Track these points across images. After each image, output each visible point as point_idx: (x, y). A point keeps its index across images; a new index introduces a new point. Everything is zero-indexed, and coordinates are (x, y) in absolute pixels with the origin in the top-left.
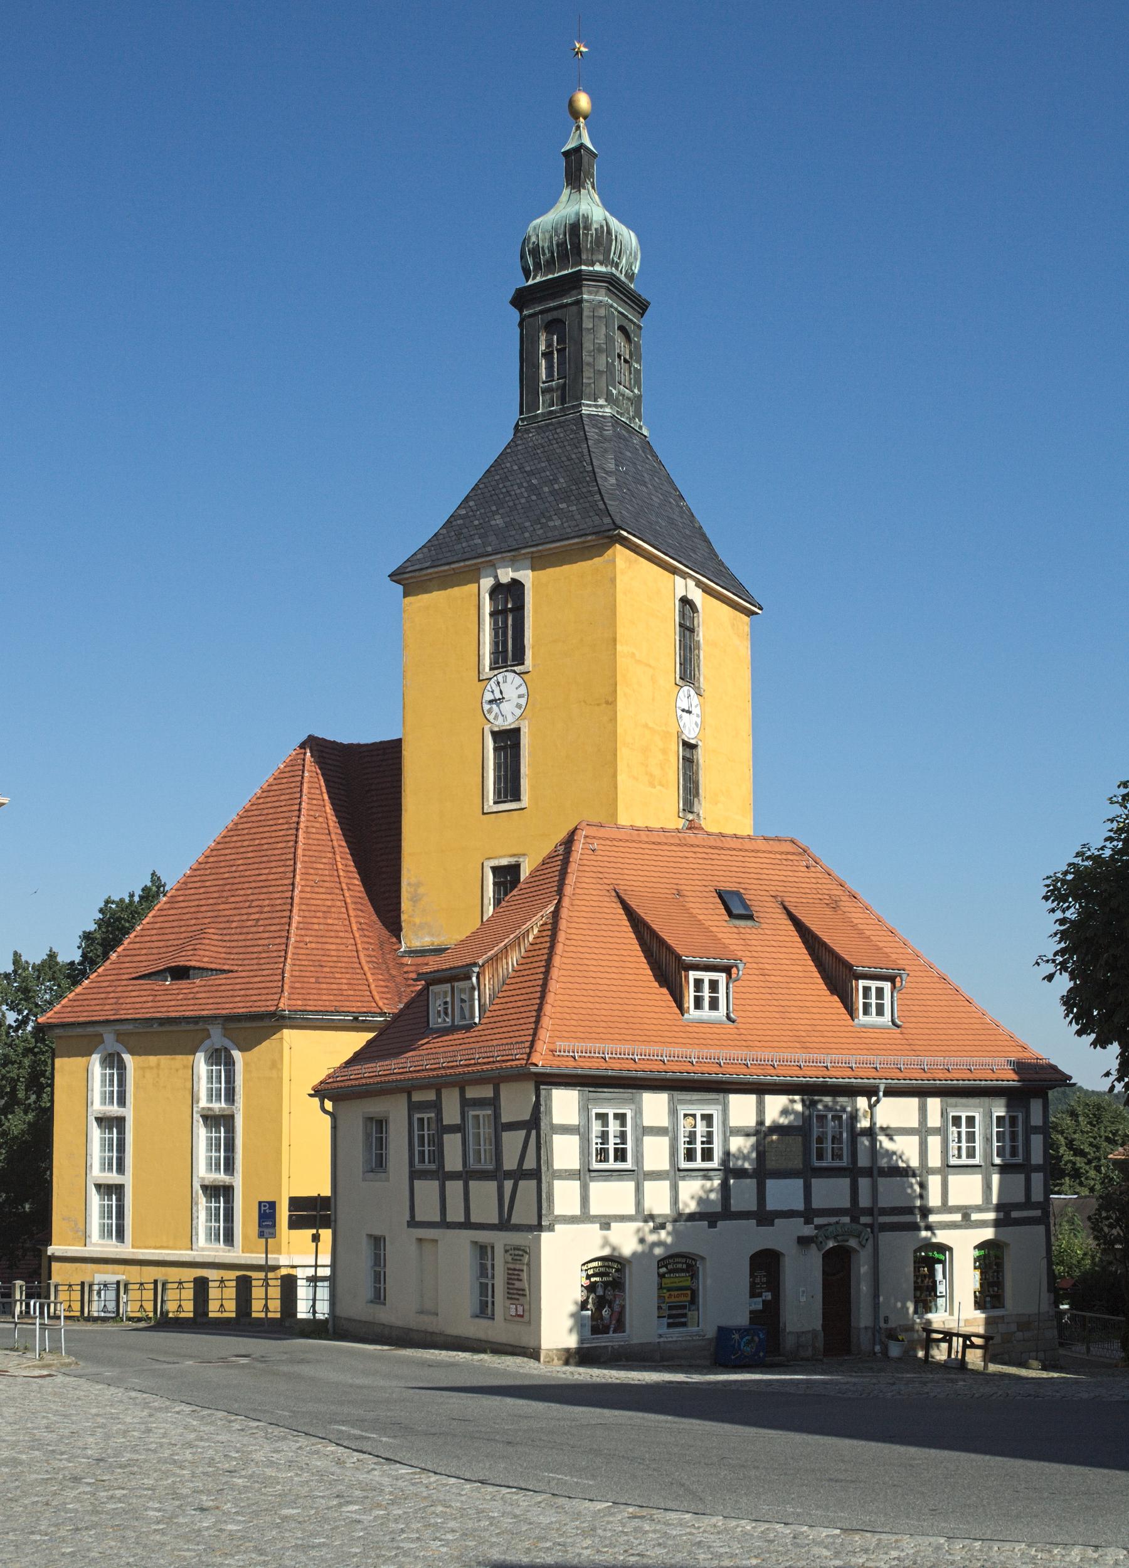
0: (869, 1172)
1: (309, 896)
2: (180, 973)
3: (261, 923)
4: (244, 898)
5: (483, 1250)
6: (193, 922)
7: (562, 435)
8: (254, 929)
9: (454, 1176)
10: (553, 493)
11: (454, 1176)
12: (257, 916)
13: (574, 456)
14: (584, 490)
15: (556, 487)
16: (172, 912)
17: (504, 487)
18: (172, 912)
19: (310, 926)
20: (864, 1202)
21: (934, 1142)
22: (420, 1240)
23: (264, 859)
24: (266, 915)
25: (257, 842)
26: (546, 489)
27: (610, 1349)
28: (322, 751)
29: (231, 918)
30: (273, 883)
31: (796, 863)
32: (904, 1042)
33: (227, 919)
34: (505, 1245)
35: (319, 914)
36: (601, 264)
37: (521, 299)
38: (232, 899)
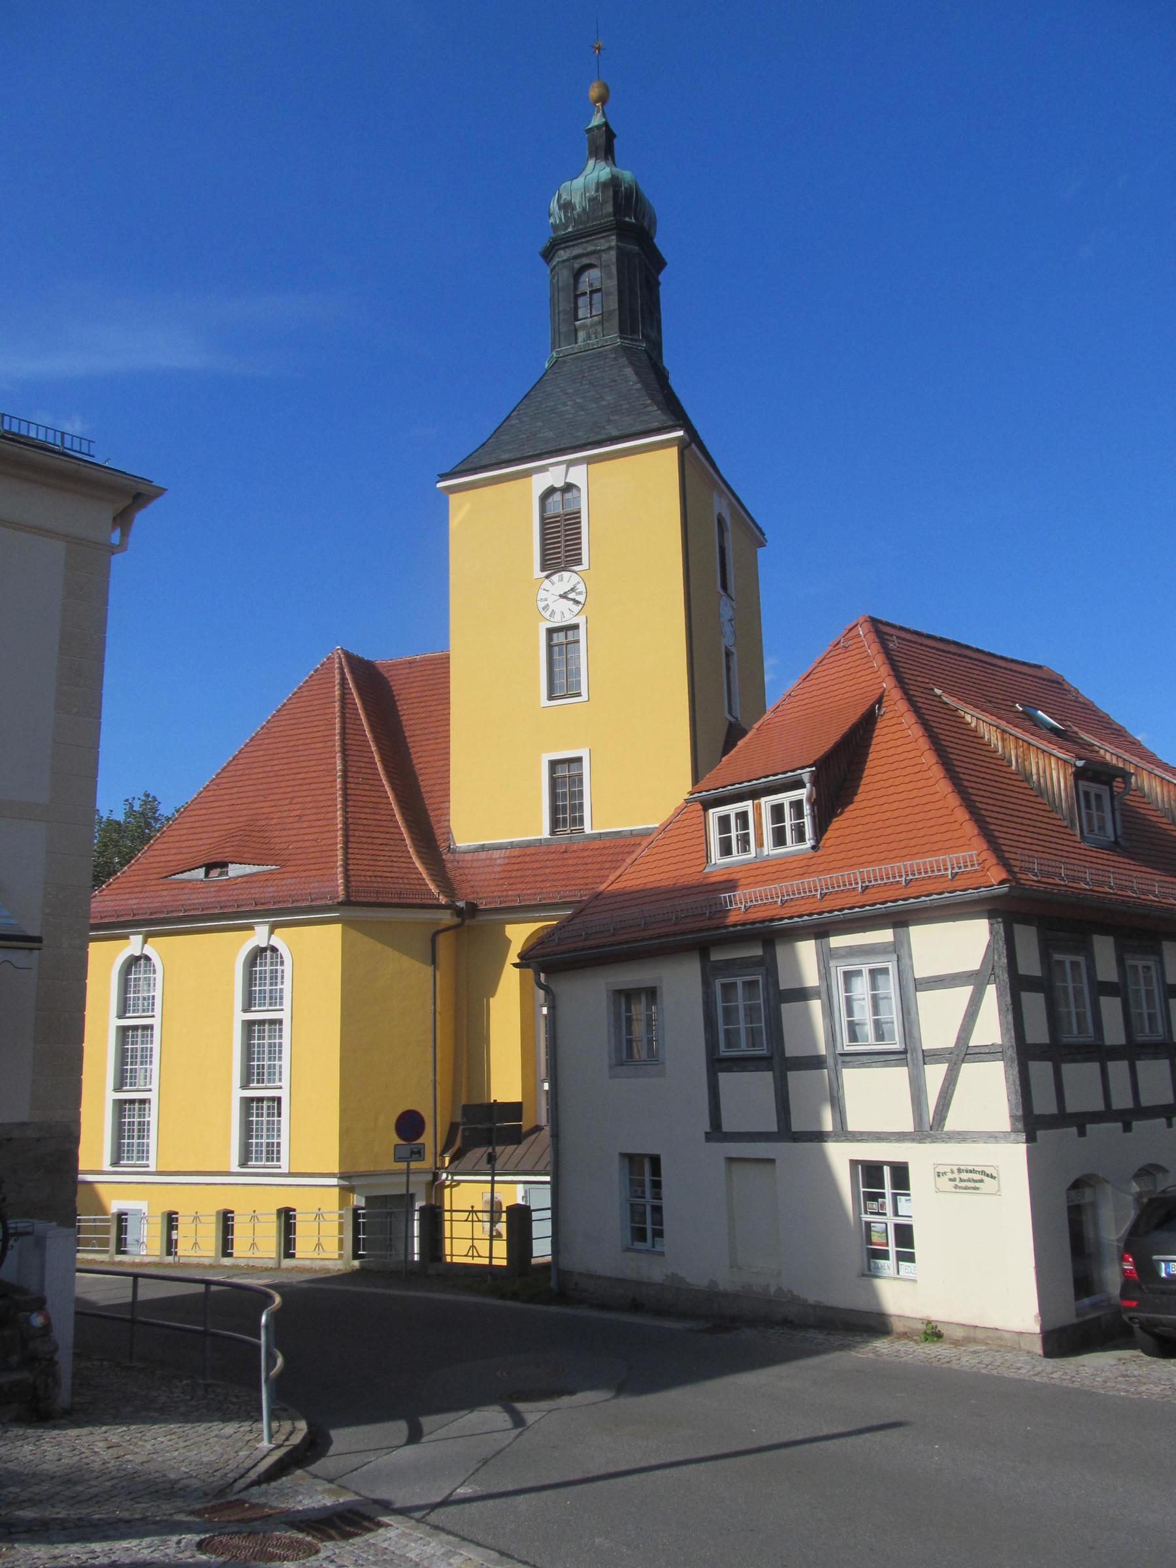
8: (297, 825)
12: (298, 813)
22: (731, 1160)
25: (291, 744)
33: (264, 816)
38: (271, 797)
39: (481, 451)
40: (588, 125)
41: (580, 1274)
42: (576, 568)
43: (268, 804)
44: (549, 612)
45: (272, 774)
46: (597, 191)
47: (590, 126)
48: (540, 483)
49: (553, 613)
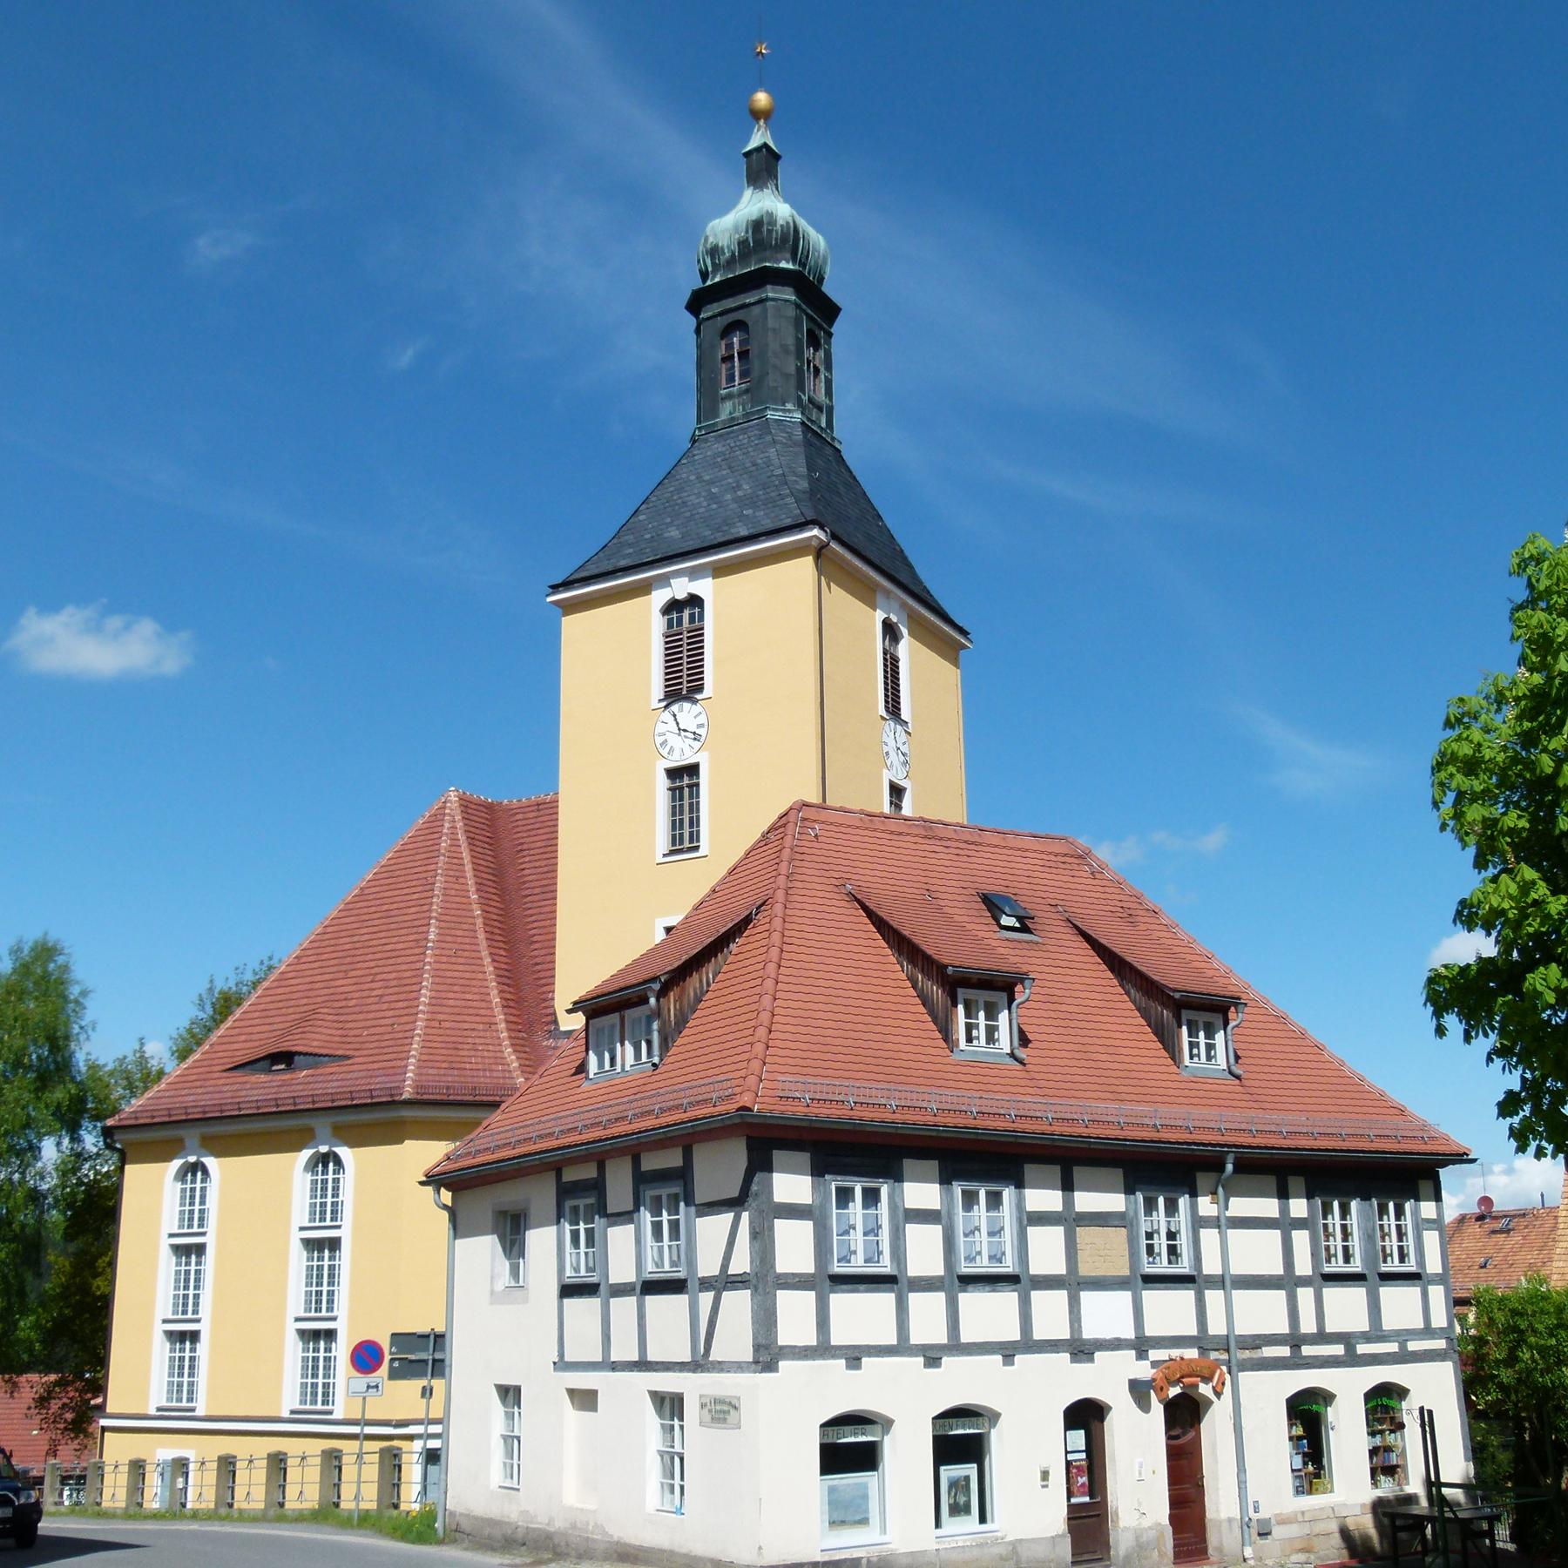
0: (1218, 1282)
1: (444, 966)
2: (285, 1058)
3: (386, 999)
4: (367, 971)
5: (670, 1405)
6: (305, 1001)
7: (746, 441)
9: (621, 1290)
10: (735, 500)
11: (621, 1290)
13: (760, 461)
14: (773, 494)
15: (740, 493)
16: (280, 991)
17: (680, 498)
18: (280, 991)
19: (445, 1002)
20: (1217, 1327)
21: (1301, 1238)
23: (393, 926)
24: (390, 991)
25: (386, 907)
26: (728, 497)
27: (864, 1561)
28: (466, 807)
29: (350, 996)
30: (403, 953)
31: (1076, 867)
32: (1247, 1097)
33: (343, 996)
34: (701, 1396)
35: (456, 988)
36: (788, 262)
37: (696, 303)
39: (601, 554)
40: (744, 147)
41: (461, 1514)
42: (699, 697)
43: (350, 981)
44: (668, 748)
45: (358, 945)
46: (747, 232)
47: (748, 148)
48: (660, 597)
49: (671, 750)
